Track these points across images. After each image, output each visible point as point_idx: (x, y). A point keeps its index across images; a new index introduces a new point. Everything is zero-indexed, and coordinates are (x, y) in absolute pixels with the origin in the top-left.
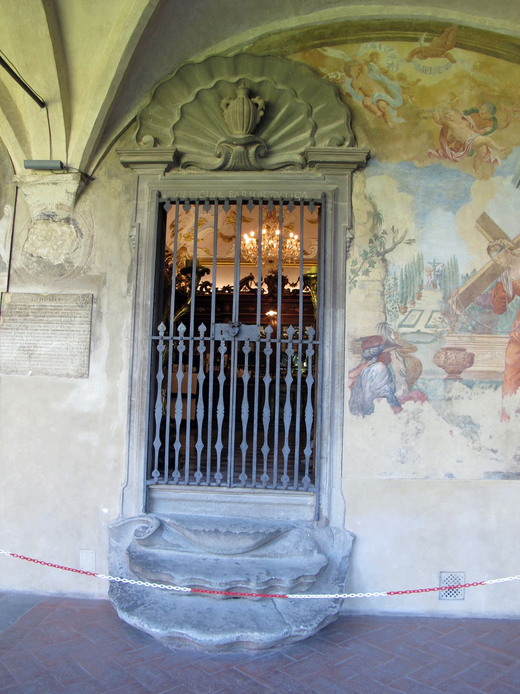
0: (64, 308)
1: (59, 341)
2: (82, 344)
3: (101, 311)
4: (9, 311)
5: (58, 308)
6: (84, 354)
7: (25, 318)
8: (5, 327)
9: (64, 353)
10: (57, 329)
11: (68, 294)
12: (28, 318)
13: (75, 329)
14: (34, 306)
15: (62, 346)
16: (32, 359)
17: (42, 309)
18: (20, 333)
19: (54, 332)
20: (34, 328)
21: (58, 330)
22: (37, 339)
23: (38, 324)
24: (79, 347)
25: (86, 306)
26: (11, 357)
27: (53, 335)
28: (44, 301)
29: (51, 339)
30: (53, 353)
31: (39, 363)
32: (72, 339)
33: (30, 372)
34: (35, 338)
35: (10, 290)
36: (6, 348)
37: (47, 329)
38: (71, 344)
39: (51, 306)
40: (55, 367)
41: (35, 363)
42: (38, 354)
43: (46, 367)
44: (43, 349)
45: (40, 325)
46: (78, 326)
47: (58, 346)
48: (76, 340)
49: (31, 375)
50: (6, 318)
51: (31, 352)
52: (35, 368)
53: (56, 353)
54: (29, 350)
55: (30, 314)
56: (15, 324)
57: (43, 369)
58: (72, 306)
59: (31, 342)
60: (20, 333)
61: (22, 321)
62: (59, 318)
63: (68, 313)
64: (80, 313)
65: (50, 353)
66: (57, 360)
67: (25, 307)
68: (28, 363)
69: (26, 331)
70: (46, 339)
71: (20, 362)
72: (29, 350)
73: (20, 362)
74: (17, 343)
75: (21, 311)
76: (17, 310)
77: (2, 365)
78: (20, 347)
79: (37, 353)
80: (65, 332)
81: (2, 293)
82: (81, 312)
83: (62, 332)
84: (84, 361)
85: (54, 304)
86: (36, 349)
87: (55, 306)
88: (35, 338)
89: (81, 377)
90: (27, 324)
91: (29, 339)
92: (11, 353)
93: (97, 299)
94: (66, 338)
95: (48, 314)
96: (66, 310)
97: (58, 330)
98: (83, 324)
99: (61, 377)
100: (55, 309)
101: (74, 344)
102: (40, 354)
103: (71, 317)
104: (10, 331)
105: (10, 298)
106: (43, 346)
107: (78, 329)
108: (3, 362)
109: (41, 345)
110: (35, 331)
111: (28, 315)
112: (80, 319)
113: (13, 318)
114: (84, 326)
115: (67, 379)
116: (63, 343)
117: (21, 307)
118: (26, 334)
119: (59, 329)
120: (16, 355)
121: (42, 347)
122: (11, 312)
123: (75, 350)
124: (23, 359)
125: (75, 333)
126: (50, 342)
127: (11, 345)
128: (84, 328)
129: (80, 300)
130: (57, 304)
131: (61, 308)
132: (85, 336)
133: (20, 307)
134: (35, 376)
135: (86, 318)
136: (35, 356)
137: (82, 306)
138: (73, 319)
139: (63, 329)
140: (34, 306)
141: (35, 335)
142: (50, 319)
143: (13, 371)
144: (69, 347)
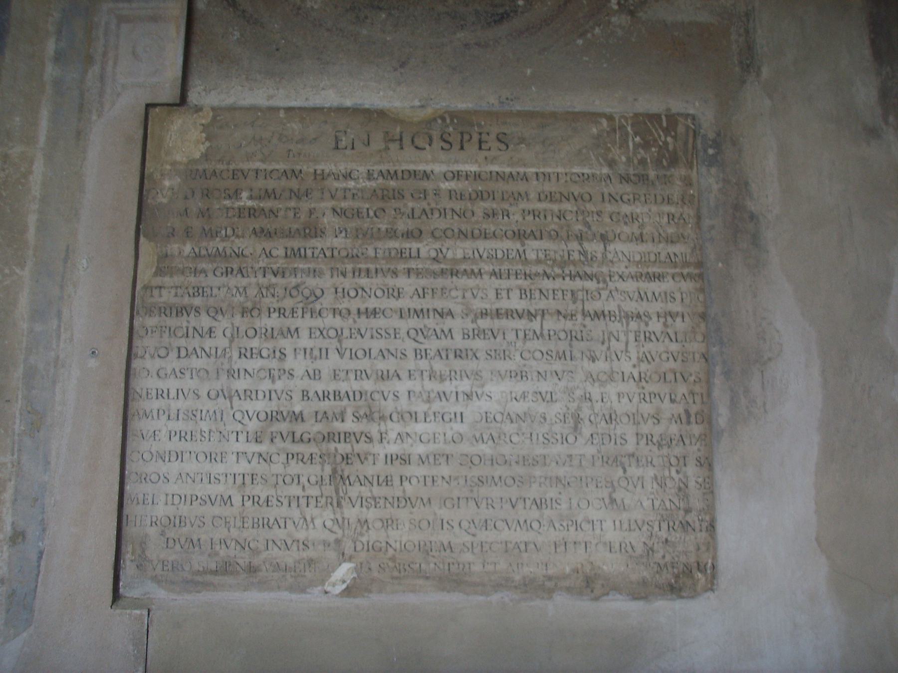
0: (534, 187)
1: (521, 375)
2: (664, 389)
3: (751, 206)
4: (196, 204)
5: (501, 186)
6: (678, 450)
7: (296, 244)
8: (167, 297)
9: (557, 449)
10: (504, 304)
11: (554, 115)
12: (317, 243)
13: (612, 306)
14: (348, 176)
15: (541, 408)
16: (354, 491)
17: (399, 195)
18: (270, 334)
19: (484, 323)
20: (354, 305)
21: (510, 314)
22: (381, 365)
23: (378, 281)
24: (647, 408)
25: (667, 180)
26: (211, 479)
27: (478, 344)
28: (409, 151)
29: (471, 365)
30: (486, 449)
31: (403, 514)
32: (602, 365)
33: (344, 571)
34: (364, 364)
35: (193, 97)
36: (179, 426)
37: (439, 304)
38: (595, 391)
39: (457, 175)
40: (506, 534)
41: (371, 514)
42: (391, 459)
43: (444, 537)
44: (420, 427)
45: (391, 281)
46: (630, 286)
47: (518, 407)
48: (626, 366)
49: (348, 592)
50: (174, 247)
51: (343, 448)
52: (371, 548)
53: (506, 449)
54: (329, 437)
55: (328, 220)
56: (235, 281)
57: (425, 549)
58: (585, 178)
59: (343, 387)
60: (270, 334)
61: (280, 263)
62: (512, 245)
63: (561, 215)
64: (633, 218)
65: (465, 448)
66: (514, 492)
67: (294, 184)
68: (328, 515)
69: (304, 323)
70: (439, 366)
71: (272, 513)
72: (329, 437)
73: (272, 513)
74: (248, 394)
75: (267, 204)
76: (245, 201)
77: (152, 531)
78: (272, 417)
79: (380, 450)
80: (550, 324)
81: (148, 106)
82: (638, 209)
83: (536, 325)
84: (682, 490)
85: (473, 168)
86: (374, 429)
87: (477, 176)
88: (364, 364)
89: (674, 590)
90: (312, 282)
91: (326, 366)
92: (210, 457)
93: (716, 144)
94: (562, 356)
95: (439, 223)
96: (550, 197)
97: (510, 314)
98: (659, 277)
99: (550, 593)
100: (480, 196)
101: (612, 390)
102: (405, 460)
103: (580, 238)
104: (205, 322)
105: (195, 134)
106: (421, 407)
107: (631, 306)
108: (161, 510)
109: (403, 404)
110: (363, 322)
111: (313, 230)
112: (635, 250)
113: (217, 244)
114: (667, 285)
115: (584, 605)
116: (544, 387)
117: (271, 184)
118: (304, 341)
119: (516, 303)
120: (243, 467)
121: (414, 416)
122: (206, 214)
123: (626, 429)
124: (295, 490)
125: (615, 326)
126: (465, 385)
127: (208, 405)
128: (668, 296)
129: (624, 143)
130: (495, 168)
131: (521, 187)
132: (674, 347)
133: (261, 183)
134: (375, 597)
135: (670, 241)
136: (370, 470)
137: (643, 178)
138: (594, 247)
139: (542, 304)
140: (348, 176)
141: (367, 343)
142: (458, 249)
143: (226, 568)
144: (586, 412)
